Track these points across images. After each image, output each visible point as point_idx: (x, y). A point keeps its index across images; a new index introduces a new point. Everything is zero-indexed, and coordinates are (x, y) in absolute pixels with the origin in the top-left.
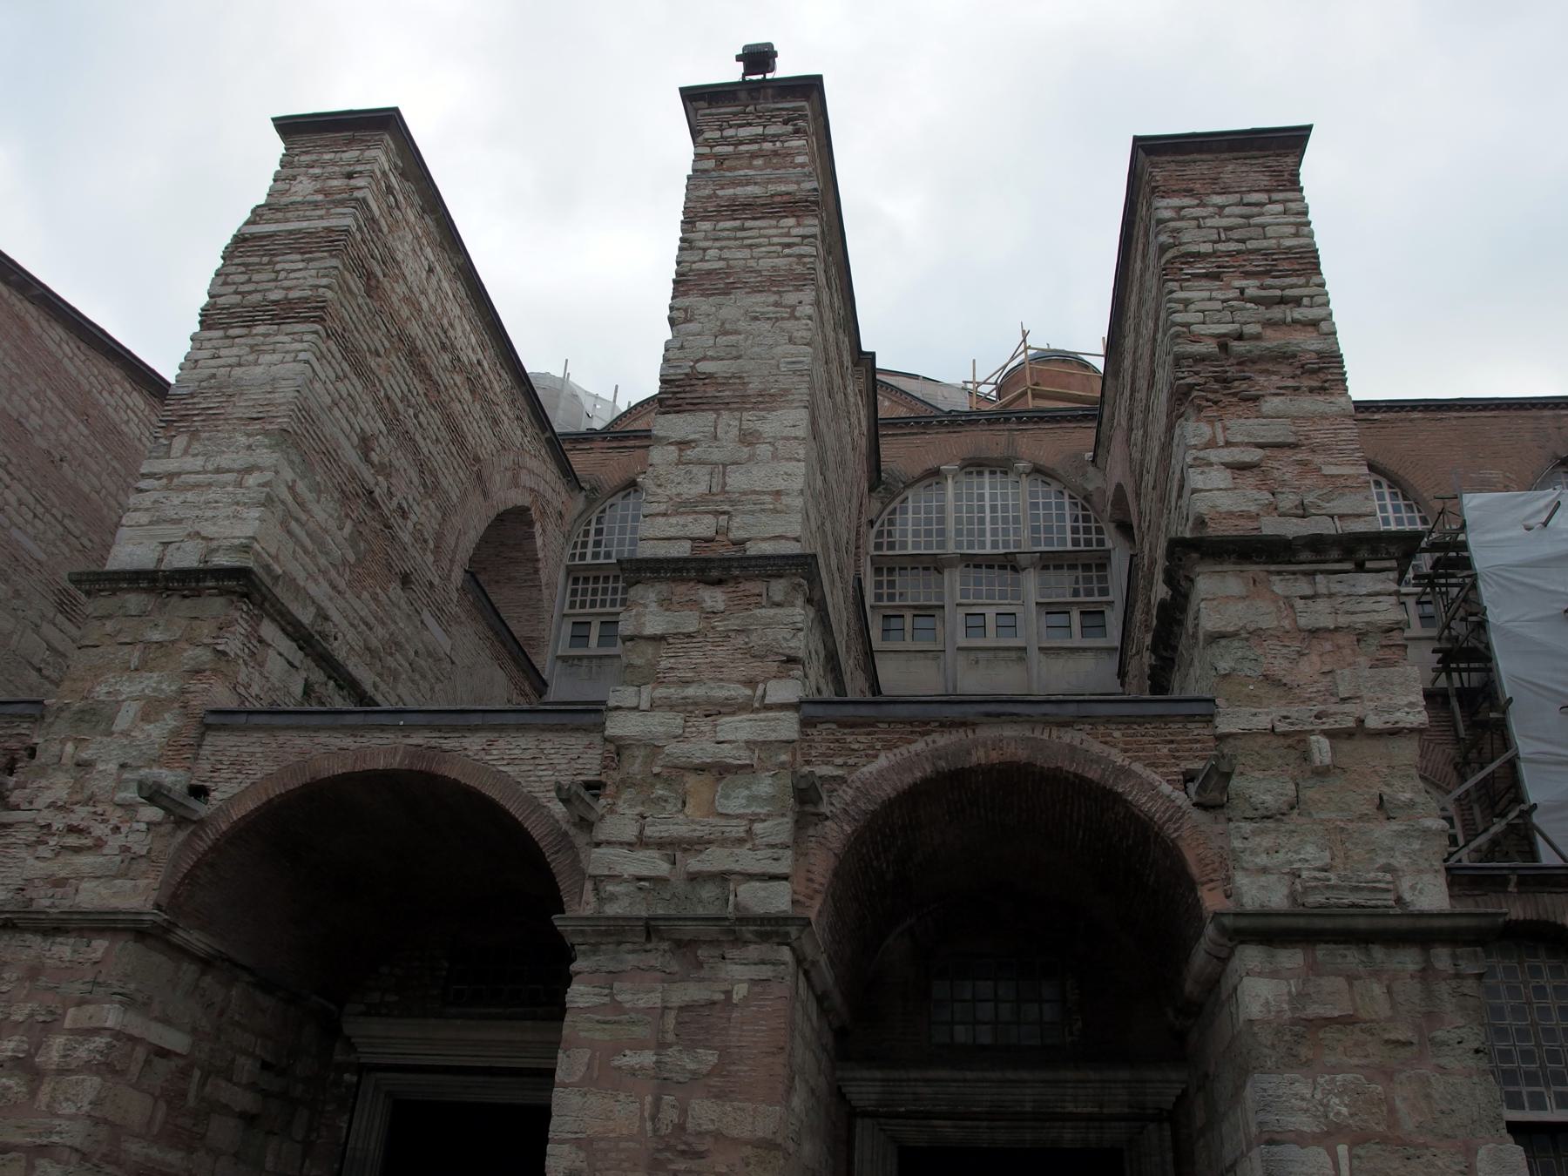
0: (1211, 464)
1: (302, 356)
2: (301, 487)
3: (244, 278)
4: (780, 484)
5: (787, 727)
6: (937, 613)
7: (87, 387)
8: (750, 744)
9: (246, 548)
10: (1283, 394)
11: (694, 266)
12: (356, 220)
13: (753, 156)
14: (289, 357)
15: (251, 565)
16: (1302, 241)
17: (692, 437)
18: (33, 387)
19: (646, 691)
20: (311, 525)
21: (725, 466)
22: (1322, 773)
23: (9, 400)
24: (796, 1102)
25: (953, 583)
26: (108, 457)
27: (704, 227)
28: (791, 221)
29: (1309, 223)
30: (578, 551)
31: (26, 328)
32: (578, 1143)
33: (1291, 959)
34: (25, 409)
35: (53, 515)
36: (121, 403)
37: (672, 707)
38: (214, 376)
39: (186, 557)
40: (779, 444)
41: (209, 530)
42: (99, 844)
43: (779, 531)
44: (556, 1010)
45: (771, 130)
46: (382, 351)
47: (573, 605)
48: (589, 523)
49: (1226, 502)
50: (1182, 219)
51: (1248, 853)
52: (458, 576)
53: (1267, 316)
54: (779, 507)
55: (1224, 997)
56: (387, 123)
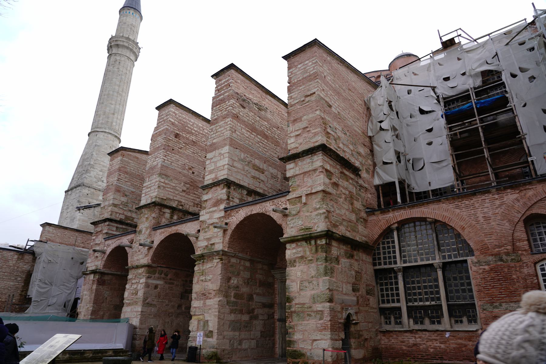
1: (161, 157)
4: (224, 163)
5: (222, 214)
8: (217, 218)
9: (156, 197)
12: (168, 125)
13: (224, 87)
18: (142, 168)
19: (204, 211)
20: (172, 187)
22: (305, 204)
23: (138, 172)
31: (138, 158)
32: (196, 293)
33: (294, 245)
34: (142, 172)
39: (149, 202)
41: (152, 195)
44: (193, 272)
45: (227, 79)
46: (183, 147)
49: (293, 146)
50: (293, 74)
56: (171, 102)
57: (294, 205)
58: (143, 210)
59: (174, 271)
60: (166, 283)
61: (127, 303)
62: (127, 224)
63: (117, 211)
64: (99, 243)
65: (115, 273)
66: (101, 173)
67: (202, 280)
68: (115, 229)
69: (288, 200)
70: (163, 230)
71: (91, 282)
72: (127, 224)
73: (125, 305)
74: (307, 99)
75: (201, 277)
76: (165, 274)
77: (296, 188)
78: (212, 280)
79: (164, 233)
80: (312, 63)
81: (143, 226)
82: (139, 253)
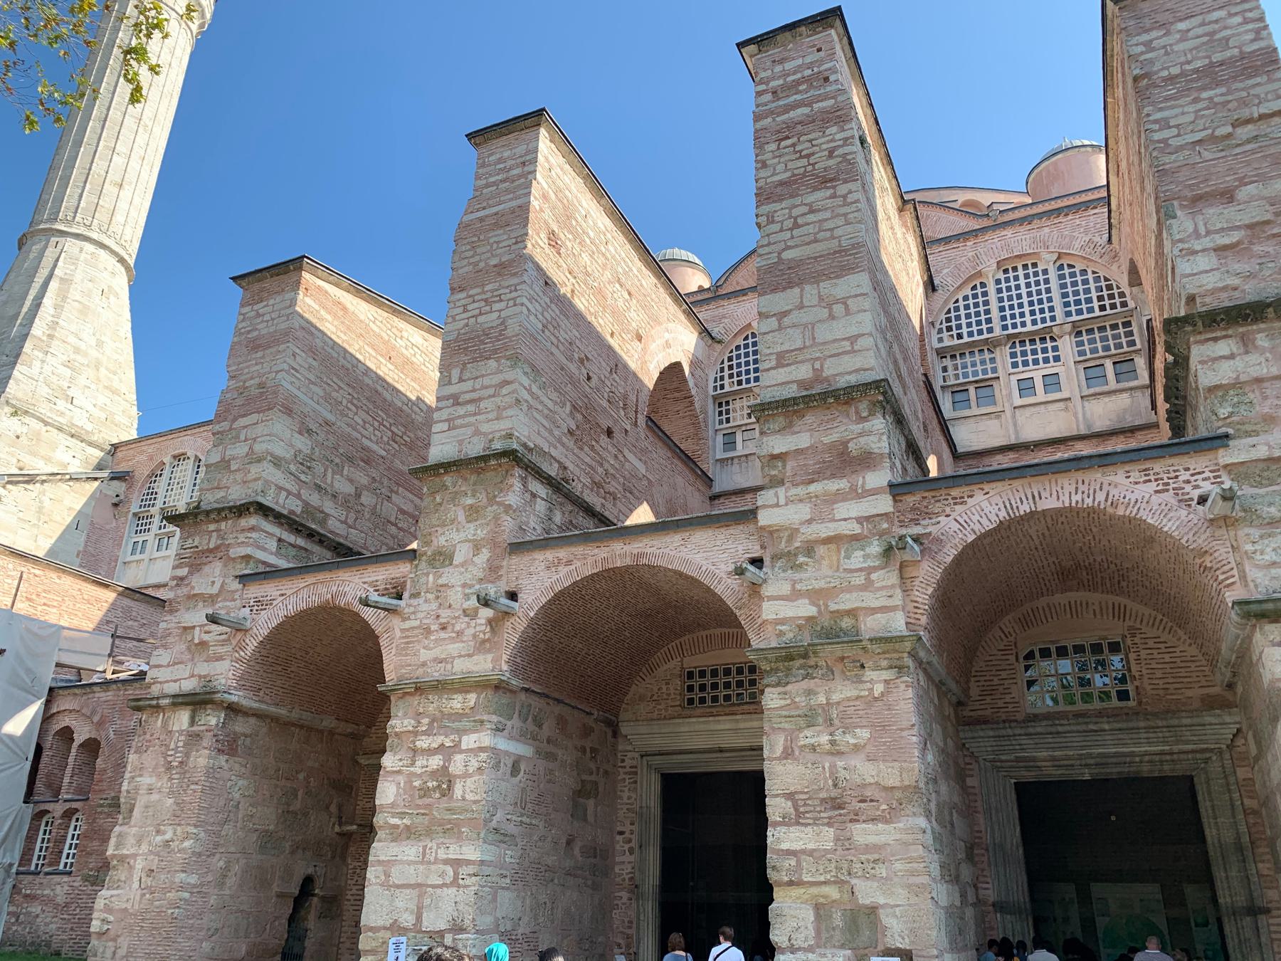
0: (1196, 252)
2: (534, 389)
3: (471, 253)
4: (853, 330)
5: (885, 504)
6: (994, 383)
7: (387, 338)
8: (860, 520)
9: (510, 436)
10: (1256, 182)
11: (768, 180)
14: (511, 303)
15: (515, 447)
16: (1262, 44)
17: (787, 308)
21: (813, 325)
24: (930, 758)
25: (1003, 356)
26: (408, 380)
27: (770, 149)
28: (834, 129)
29: (1266, 27)
30: (719, 383)
31: (344, 309)
35: (384, 426)
36: (409, 344)
37: (801, 501)
38: (467, 325)
39: (475, 448)
40: (849, 302)
42: (460, 633)
43: (858, 366)
45: (808, 60)
47: (721, 422)
48: (722, 363)
49: (1211, 281)
50: (1153, 50)
51: (1258, 553)
52: (642, 420)
53: (1236, 117)
54: (856, 348)
55: (1255, 659)
57: (1260, 485)
58: (448, 479)
59: (558, 709)
60: (538, 752)
61: (396, 827)
62: (311, 535)
63: (282, 483)
64: (215, 590)
65: (273, 709)
66: (68, 372)
67: (813, 748)
68: (273, 545)
69: (1225, 466)
70: (562, 553)
71: (179, 741)
72: (311, 535)
73: (381, 834)
74: (1245, 132)
75: (808, 732)
76: (534, 720)
77: (1258, 427)
78: (869, 748)
79: (569, 563)
80: (1245, 19)
81: (456, 537)
82: (443, 635)
